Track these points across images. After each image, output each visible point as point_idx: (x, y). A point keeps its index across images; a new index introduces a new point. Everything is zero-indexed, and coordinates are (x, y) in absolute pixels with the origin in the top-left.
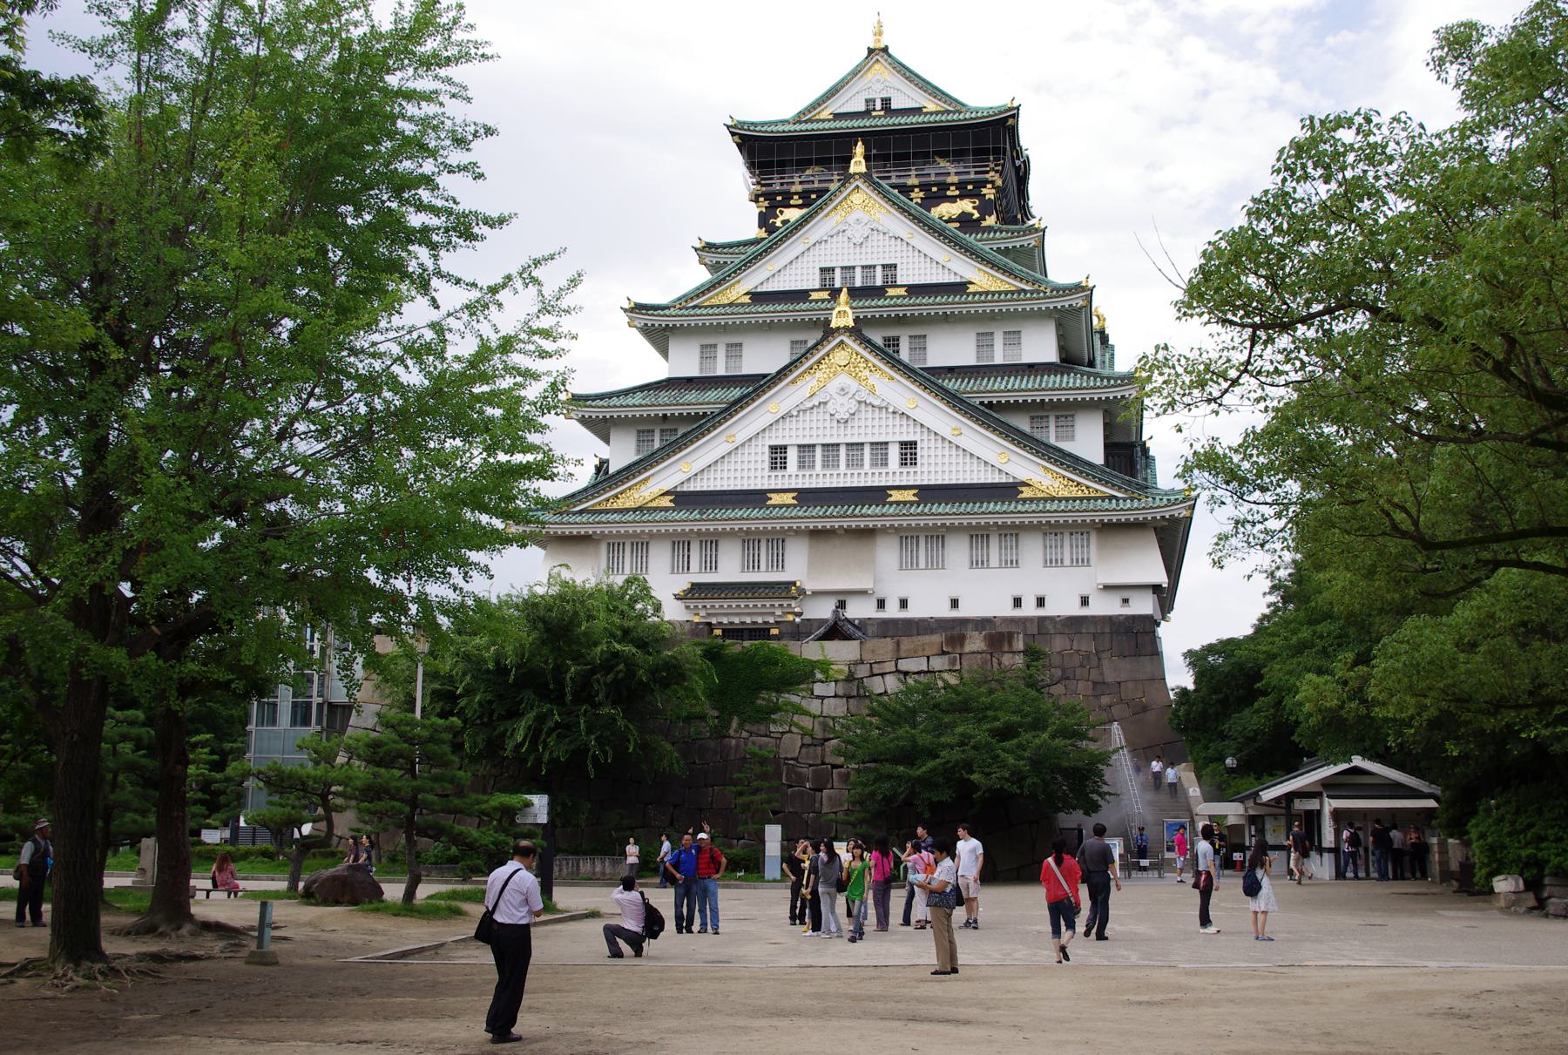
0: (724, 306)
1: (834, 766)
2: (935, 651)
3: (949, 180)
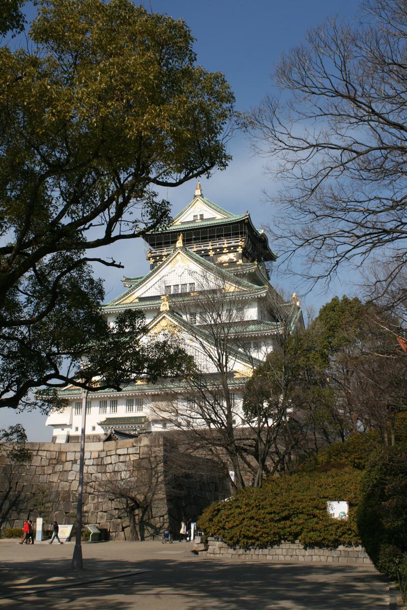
0: (128, 304)
1: (90, 494)
2: (131, 445)
3: (224, 246)
